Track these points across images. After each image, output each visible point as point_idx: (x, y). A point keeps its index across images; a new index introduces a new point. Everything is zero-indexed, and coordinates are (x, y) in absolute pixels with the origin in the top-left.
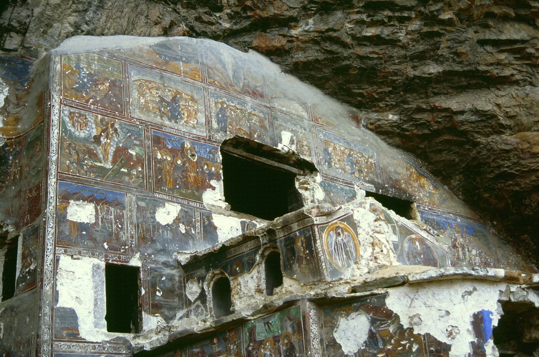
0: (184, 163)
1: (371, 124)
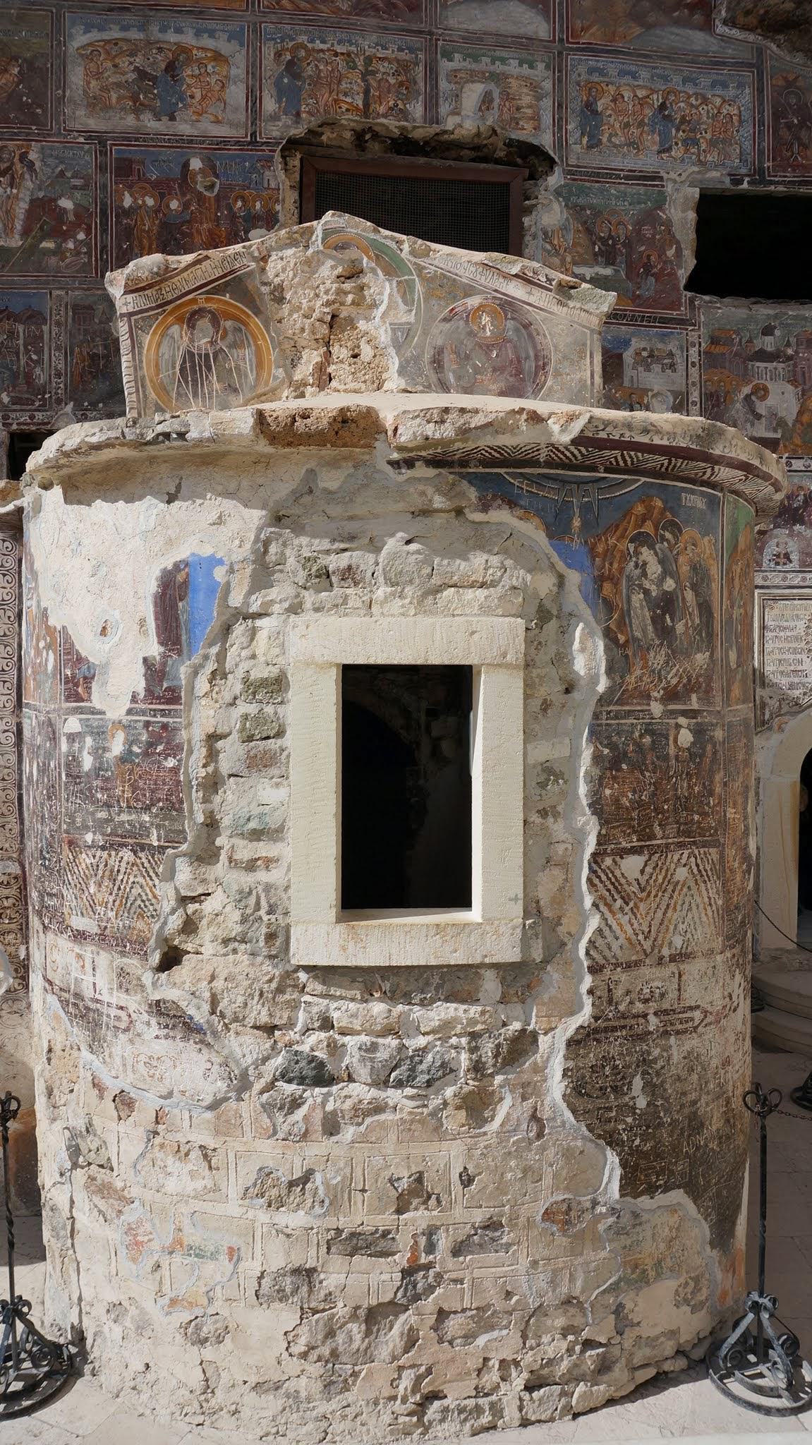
0: (186, 206)
1: (747, 13)
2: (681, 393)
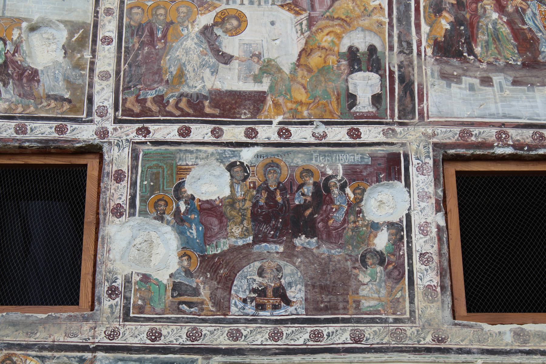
2: (83, 25)
